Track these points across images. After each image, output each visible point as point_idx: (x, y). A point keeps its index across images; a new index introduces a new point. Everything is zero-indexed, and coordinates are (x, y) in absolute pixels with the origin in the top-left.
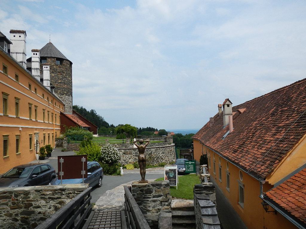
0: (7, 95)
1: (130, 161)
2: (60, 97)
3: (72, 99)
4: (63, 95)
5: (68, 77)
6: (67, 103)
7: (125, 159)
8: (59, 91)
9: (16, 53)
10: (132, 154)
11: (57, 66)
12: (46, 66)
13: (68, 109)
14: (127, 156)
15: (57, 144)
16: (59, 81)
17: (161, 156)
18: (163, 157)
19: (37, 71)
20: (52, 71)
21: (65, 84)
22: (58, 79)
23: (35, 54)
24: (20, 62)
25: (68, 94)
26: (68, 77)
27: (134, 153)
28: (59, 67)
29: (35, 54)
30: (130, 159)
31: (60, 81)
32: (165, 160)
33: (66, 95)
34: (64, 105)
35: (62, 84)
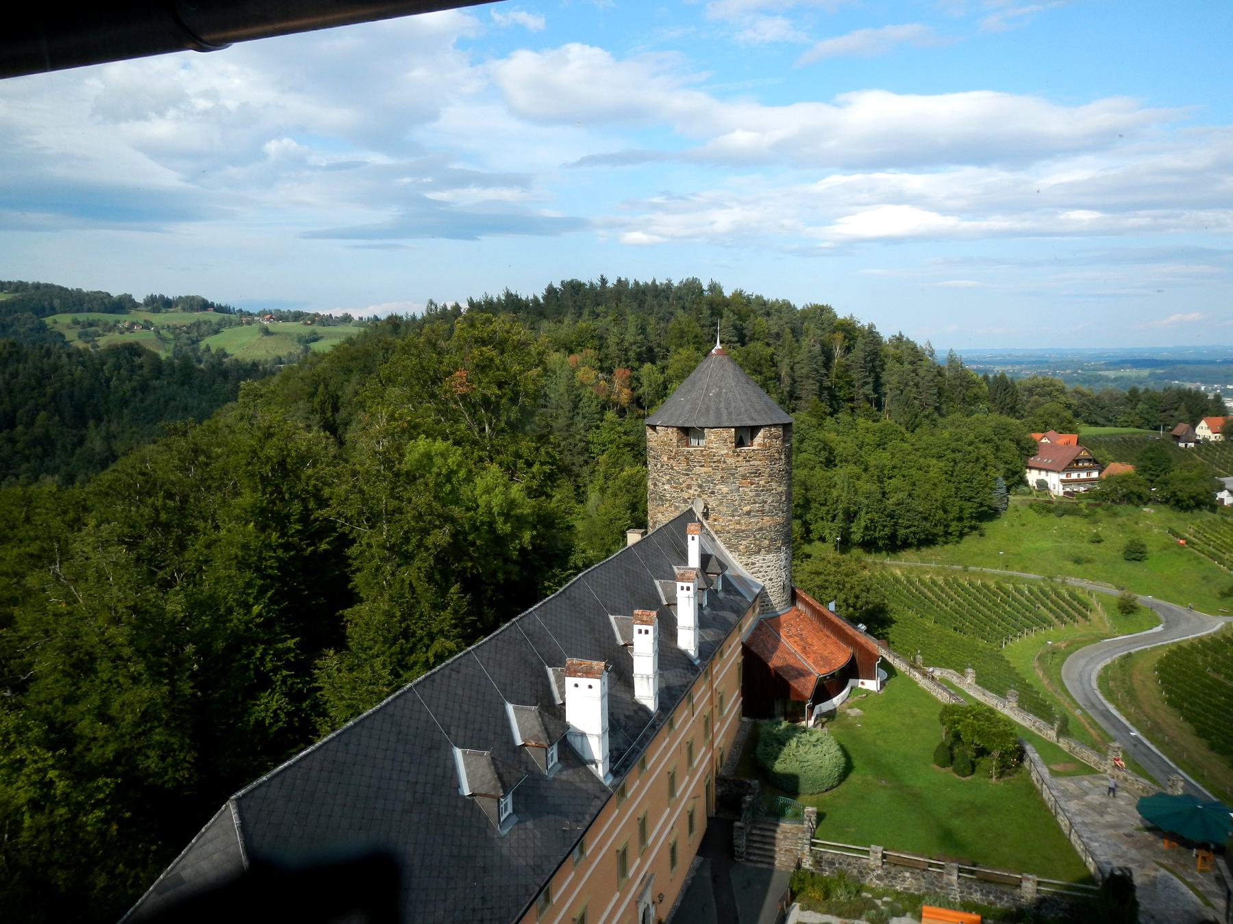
2: (747, 565)
4: (758, 552)
6: (771, 580)
8: (744, 543)
11: (738, 455)
20: (722, 477)
31: (747, 508)
33: (768, 552)
35: (755, 516)
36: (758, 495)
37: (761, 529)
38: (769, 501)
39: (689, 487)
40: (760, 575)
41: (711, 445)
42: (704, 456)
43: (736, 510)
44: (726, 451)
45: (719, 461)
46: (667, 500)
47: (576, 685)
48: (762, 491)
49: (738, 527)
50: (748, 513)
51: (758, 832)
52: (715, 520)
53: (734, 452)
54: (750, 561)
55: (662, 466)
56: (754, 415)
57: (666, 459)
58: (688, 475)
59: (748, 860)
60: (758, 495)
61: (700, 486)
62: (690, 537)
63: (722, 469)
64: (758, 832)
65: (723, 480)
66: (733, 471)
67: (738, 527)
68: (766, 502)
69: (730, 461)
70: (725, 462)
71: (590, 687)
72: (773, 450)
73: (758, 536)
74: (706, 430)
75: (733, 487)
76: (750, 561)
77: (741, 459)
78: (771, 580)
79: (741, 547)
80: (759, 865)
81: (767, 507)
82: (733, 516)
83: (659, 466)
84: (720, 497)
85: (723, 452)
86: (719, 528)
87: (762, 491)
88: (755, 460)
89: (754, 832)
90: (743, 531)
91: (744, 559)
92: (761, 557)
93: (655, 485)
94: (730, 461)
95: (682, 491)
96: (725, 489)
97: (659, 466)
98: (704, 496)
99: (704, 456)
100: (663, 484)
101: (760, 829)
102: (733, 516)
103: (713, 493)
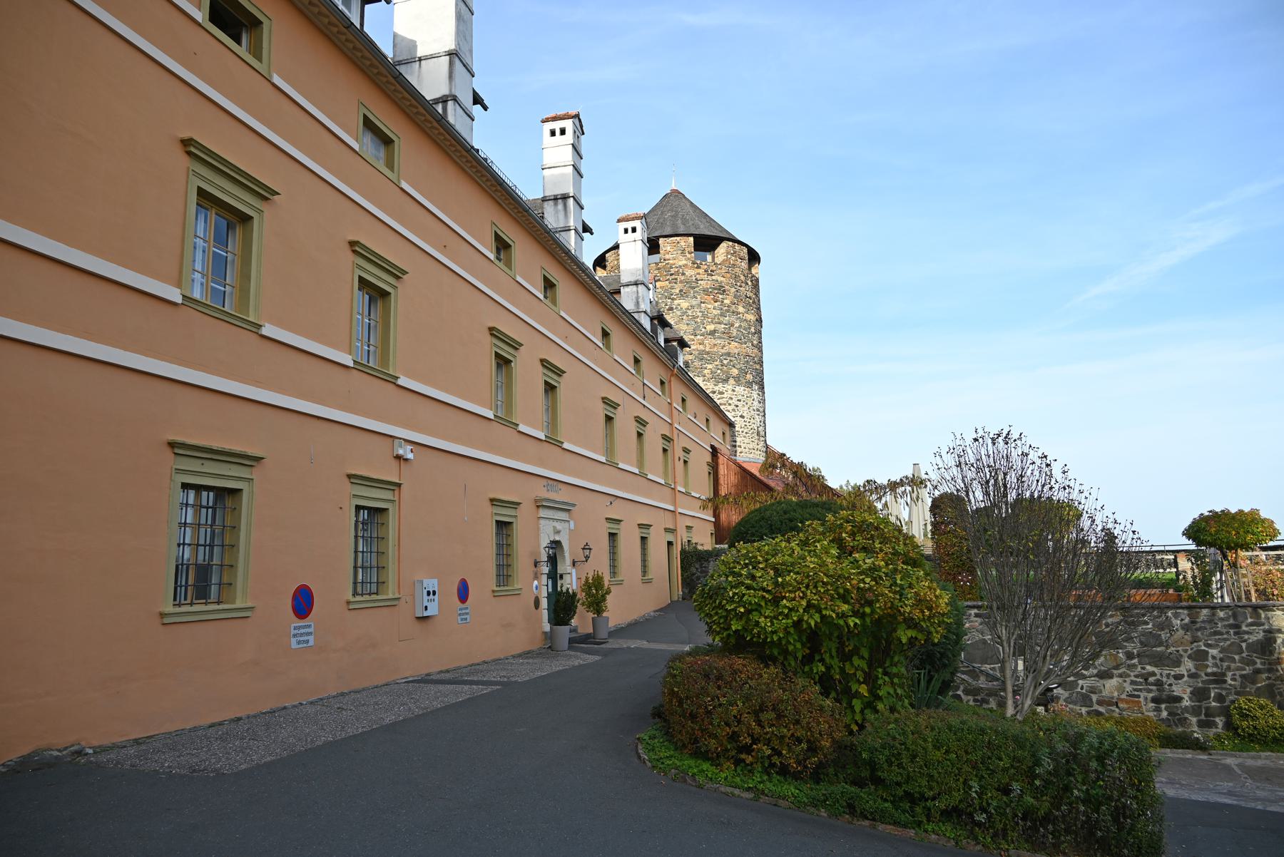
0: (559, 372)
3: (763, 401)
4: (726, 381)
5: (741, 309)
8: (710, 366)
20: (681, 291)
22: (704, 316)
26: (741, 309)
31: (711, 327)
34: (731, 425)
35: (720, 338)
36: (722, 315)
38: (737, 325)
41: (667, 257)
44: (684, 262)
48: (728, 311)
49: (701, 347)
50: (713, 333)
53: (694, 263)
60: (722, 315)
63: (681, 282)
65: (682, 294)
66: (694, 285)
68: (732, 325)
69: (689, 272)
70: (683, 274)
72: (737, 270)
74: (661, 241)
75: (694, 302)
76: (716, 388)
77: (701, 271)
79: (706, 371)
81: (734, 332)
84: (679, 313)
85: (681, 263)
87: (728, 311)
88: (718, 274)
90: (708, 353)
92: (730, 387)
94: (689, 272)
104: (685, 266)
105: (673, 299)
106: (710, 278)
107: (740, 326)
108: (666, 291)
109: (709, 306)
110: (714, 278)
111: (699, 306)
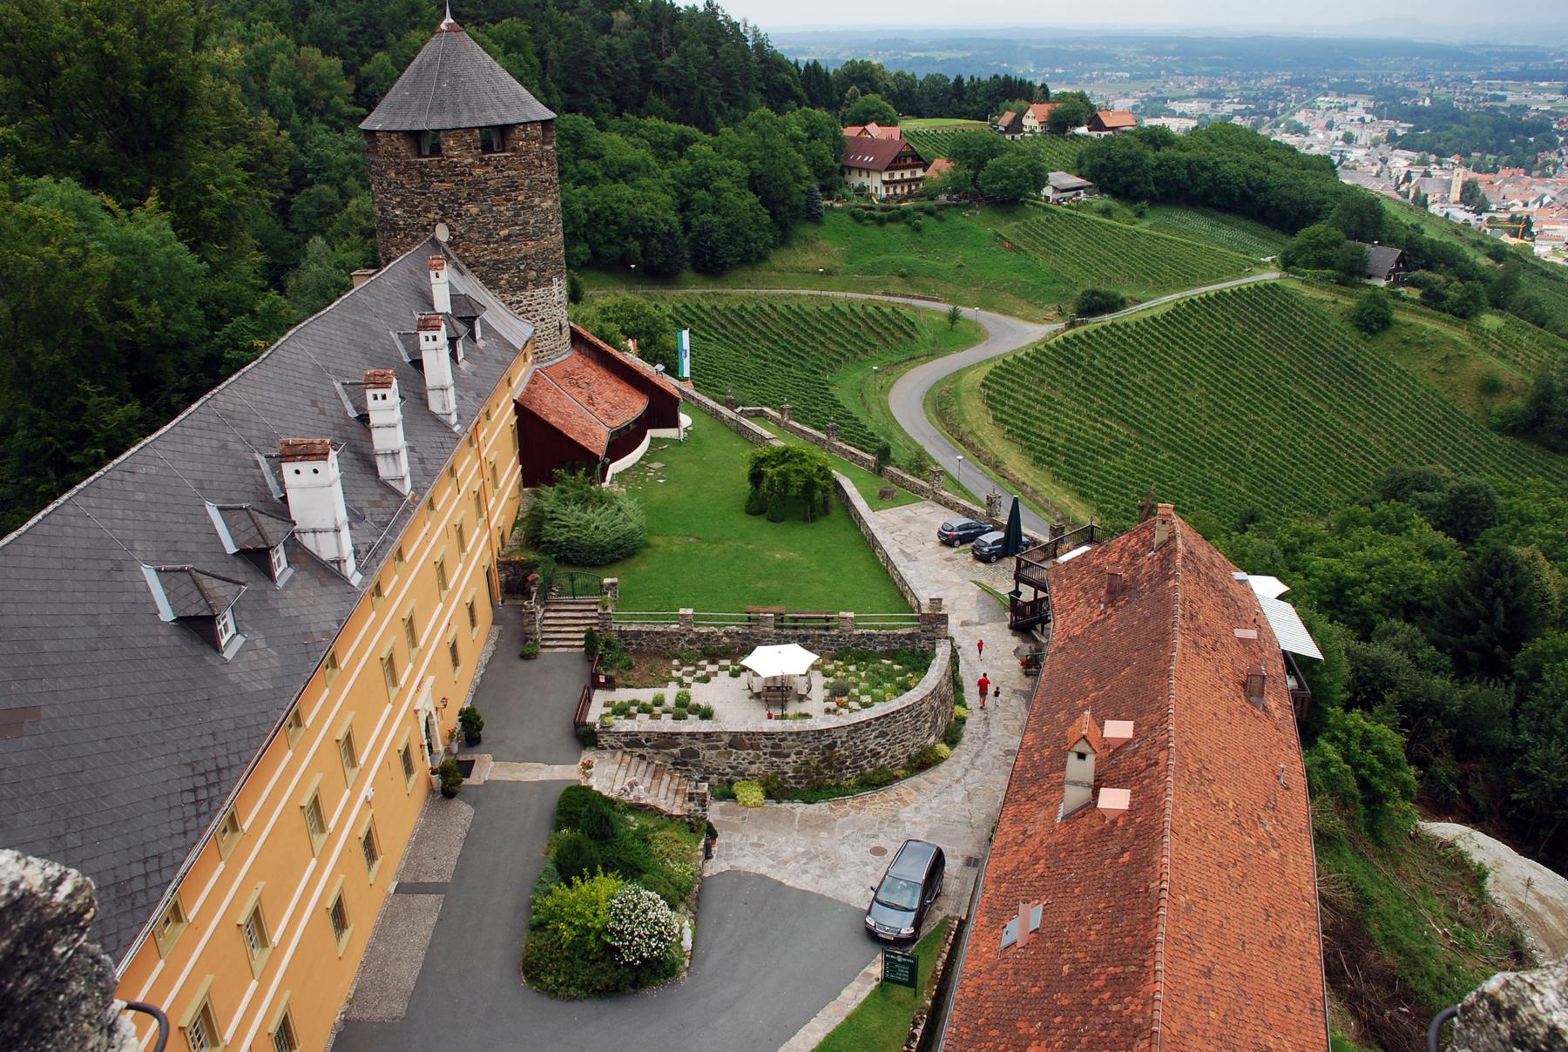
1: (754, 768)
2: (511, 304)
4: (523, 288)
6: (542, 320)
7: (735, 764)
8: (506, 276)
9: (314, 532)
10: (758, 748)
11: (487, 165)
12: (430, 334)
13: (549, 342)
14: (743, 753)
15: (507, 581)
16: (502, 233)
17: (872, 746)
18: (880, 749)
19: (394, 459)
20: (469, 194)
21: (528, 237)
22: (497, 221)
23: (380, 397)
24: (332, 562)
25: (542, 280)
27: (765, 746)
28: (496, 167)
29: (380, 397)
30: (751, 763)
31: (504, 233)
32: (890, 754)
33: (537, 286)
35: (515, 242)
37: (525, 257)
38: (532, 221)
39: (427, 210)
40: (529, 315)
42: (442, 168)
43: (491, 235)
44: (470, 160)
45: (463, 174)
46: (400, 229)
47: (297, 472)
48: (523, 208)
49: (496, 257)
50: (507, 238)
51: (553, 614)
52: (465, 250)
53: (481, 160)
54: (514, 299)
55: (389, 185)
56: (502, 111)
57: (393, 175)
58: (424, 194)
59: (543, 647)
61: (441, 208)
62: (433, 274)
64: (553, 614)
65: (471, 199)
66: (482, 186)
67: (496, 257)
68: (528, 223)
69: (478, 172)
70: (470, 174)
71: (316, 471)
73: (522, 267)
76: (514, 299)
77: (490, 169)
78: (542, 320)
80: (557, 650)
82: (488, 244)
83: (385, 185)
86: (471, 260)
88: (510, 169)
89: (548, 615)
91: (508, 297)
93: (383, 210)
94: (478, 172)
95: (419, 216)
96: (474, 210)
97: (385, 185)
98: (449, 221)
99: (442, 168)
100: (393, 208)
101: (555, 611)
102: (488, 244)
103: (459, 215)
104: (472, 164)
105: (461, 204)
106: (500, 175)
107: (536, 221)
108: (452, 194)
109: (502, 208)
110: (505, 174)
111: (490, 210)
